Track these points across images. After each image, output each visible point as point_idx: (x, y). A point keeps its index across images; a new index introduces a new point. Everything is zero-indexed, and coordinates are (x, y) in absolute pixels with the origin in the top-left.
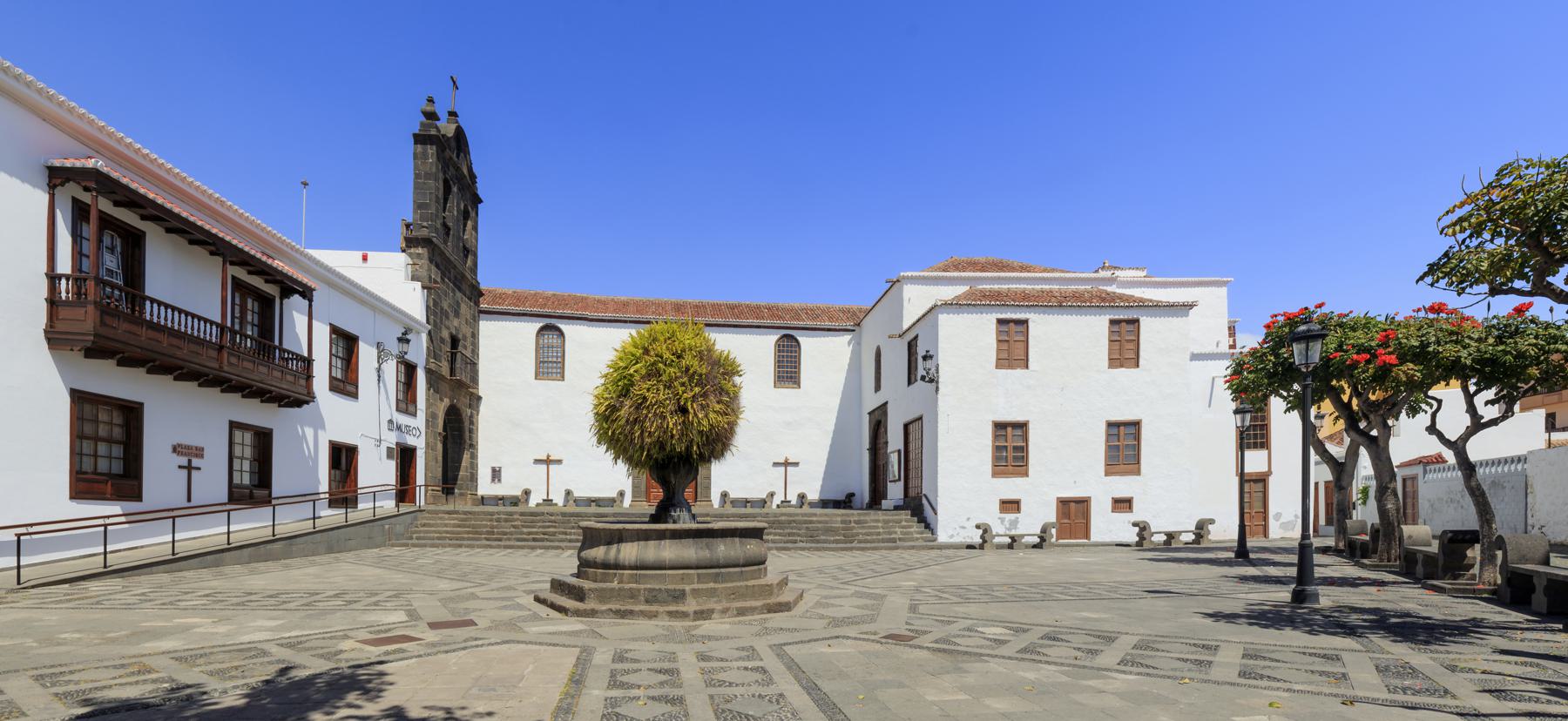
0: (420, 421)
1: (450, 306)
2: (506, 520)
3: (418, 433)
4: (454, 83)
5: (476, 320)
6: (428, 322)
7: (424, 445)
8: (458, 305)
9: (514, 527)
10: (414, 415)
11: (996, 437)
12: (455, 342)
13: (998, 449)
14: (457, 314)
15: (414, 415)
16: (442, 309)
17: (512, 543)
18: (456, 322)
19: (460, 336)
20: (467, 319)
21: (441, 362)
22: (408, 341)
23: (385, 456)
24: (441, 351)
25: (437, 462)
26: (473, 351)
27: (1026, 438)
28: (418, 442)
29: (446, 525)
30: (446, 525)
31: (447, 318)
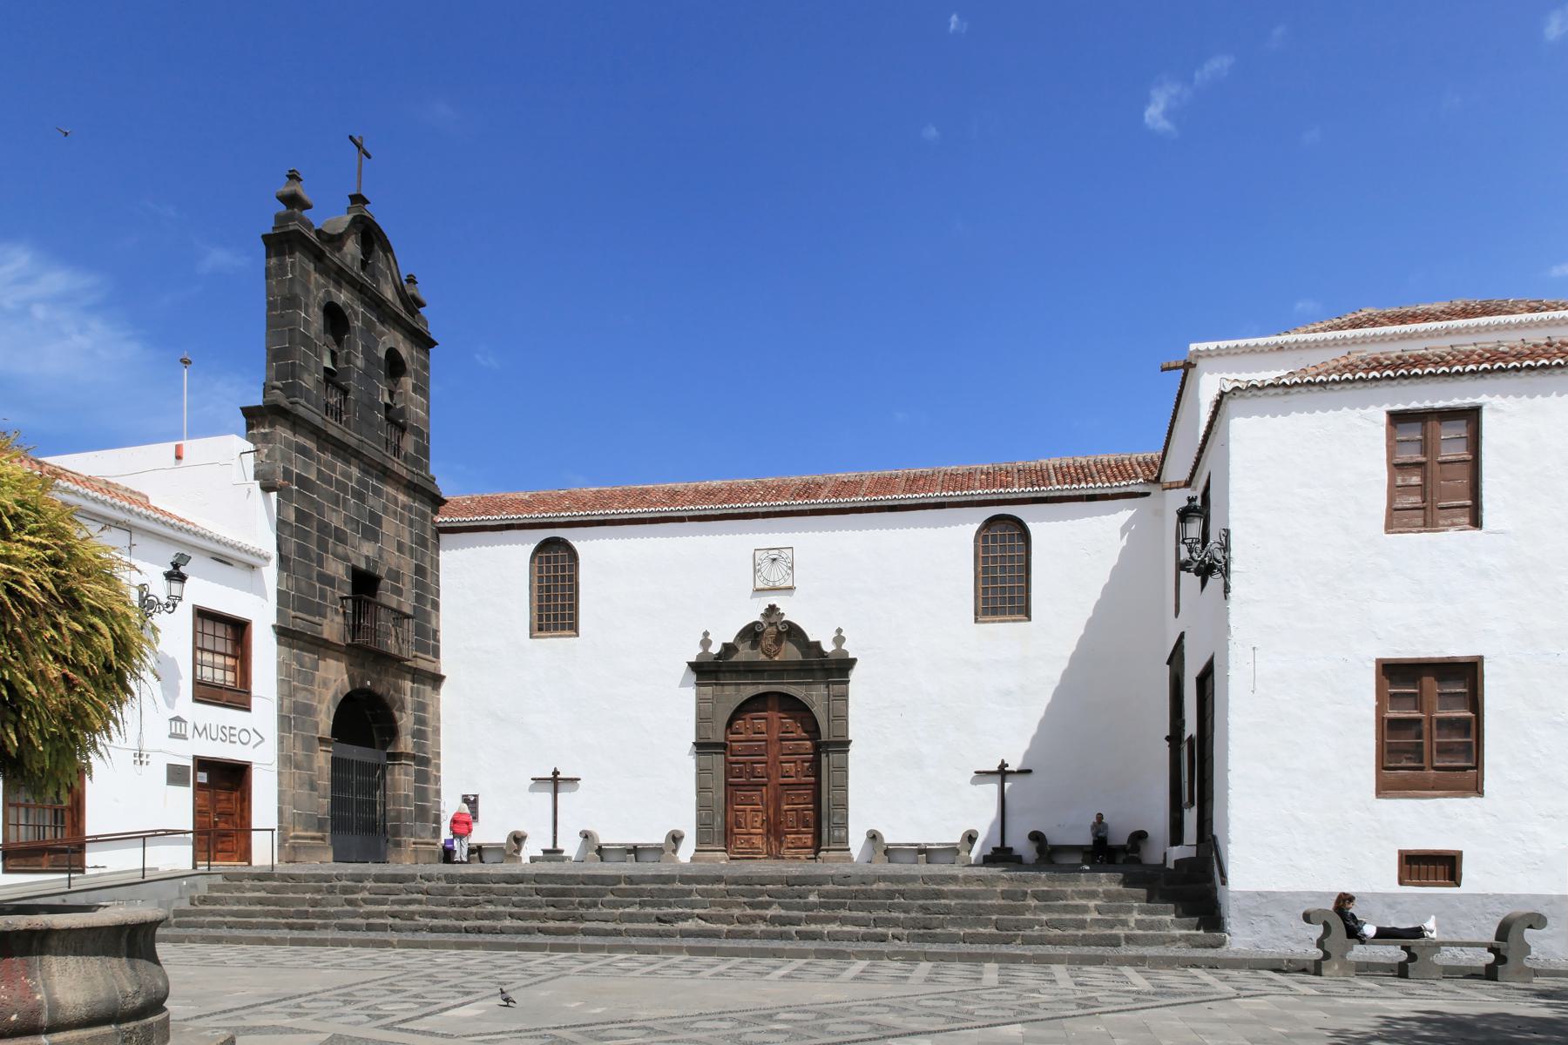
4: (359, 146)
8: (376, 519)
11: (1384, 699)
12: (364, 583)
13: (1389, 728)
14: (371, 534)
18: (368, 549)
19: (382, 571)
22: (182, 578)
27: (1475, 701)
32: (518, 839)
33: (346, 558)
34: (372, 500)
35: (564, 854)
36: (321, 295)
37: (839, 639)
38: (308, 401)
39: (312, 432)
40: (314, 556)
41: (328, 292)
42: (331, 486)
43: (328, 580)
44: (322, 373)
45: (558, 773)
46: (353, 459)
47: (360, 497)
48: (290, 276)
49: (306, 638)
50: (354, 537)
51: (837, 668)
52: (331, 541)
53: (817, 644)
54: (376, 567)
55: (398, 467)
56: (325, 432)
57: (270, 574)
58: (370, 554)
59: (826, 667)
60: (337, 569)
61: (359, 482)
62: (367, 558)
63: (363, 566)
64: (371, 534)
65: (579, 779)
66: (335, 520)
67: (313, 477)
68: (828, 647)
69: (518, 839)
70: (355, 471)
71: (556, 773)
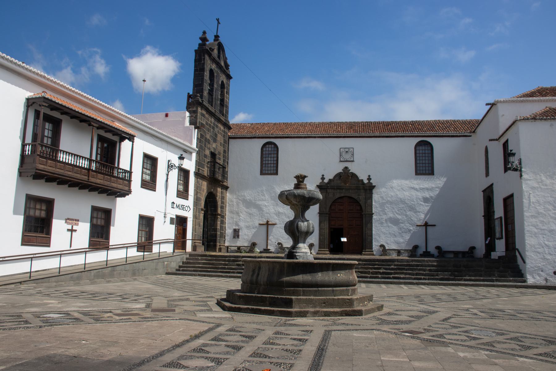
0: (190, 202)
1: (211, 136)
2: (234, 261)
3: (189, 209)
5: (226, 143)
6: (197, 147)
7: (192, 217)
8: (216, 135)
9: (238, 265)
10: (186, 197)
14: (215, 140)
15: (186, 197)
16: (206, 138)
17: (235, 275)
18: (214, 145)
20: (221, 143)
21: (204, 168)
23: (189, 220)
24: (204, 162)
25: (199, 226)
26: (224, 161)
28: (189, 215)
29: (199, 263)
30: (199, 263)
31: (209, 143)
32: (254, 245)
33: (209, 149)
34: (216, 130)
35: (270, 251)
36: (209, 67)
37: (369, 179)
38: (205, 100)
39: (205, 109)
40: (203, 149)
41: (211, 66)
42: (207, 125)
43: (205, 156)
44: (208, 90)
45: (269, 222)
46: (213, 117)
47: (213, 128)
48: (203, 62)
49: (201, 176)
50: (212, 141)
51: (369, 188)
52: (207, 143)
53: (362, 180)
54: (216, 151)
55: (222, 118)
56: (208, 109)
57: (194, 155)
58: (215, 147)
59: (365, 188)
60: (208, 152)
61: (214, 124)
62: (214, 148)
63: (213, 151)
64: (215, 140)
65: (276, 224)
66: (208, 137)
67: (205, 123)
68: (366, 181)
69: (254, 245)
70: (213, 120)
71: (268, 222)
